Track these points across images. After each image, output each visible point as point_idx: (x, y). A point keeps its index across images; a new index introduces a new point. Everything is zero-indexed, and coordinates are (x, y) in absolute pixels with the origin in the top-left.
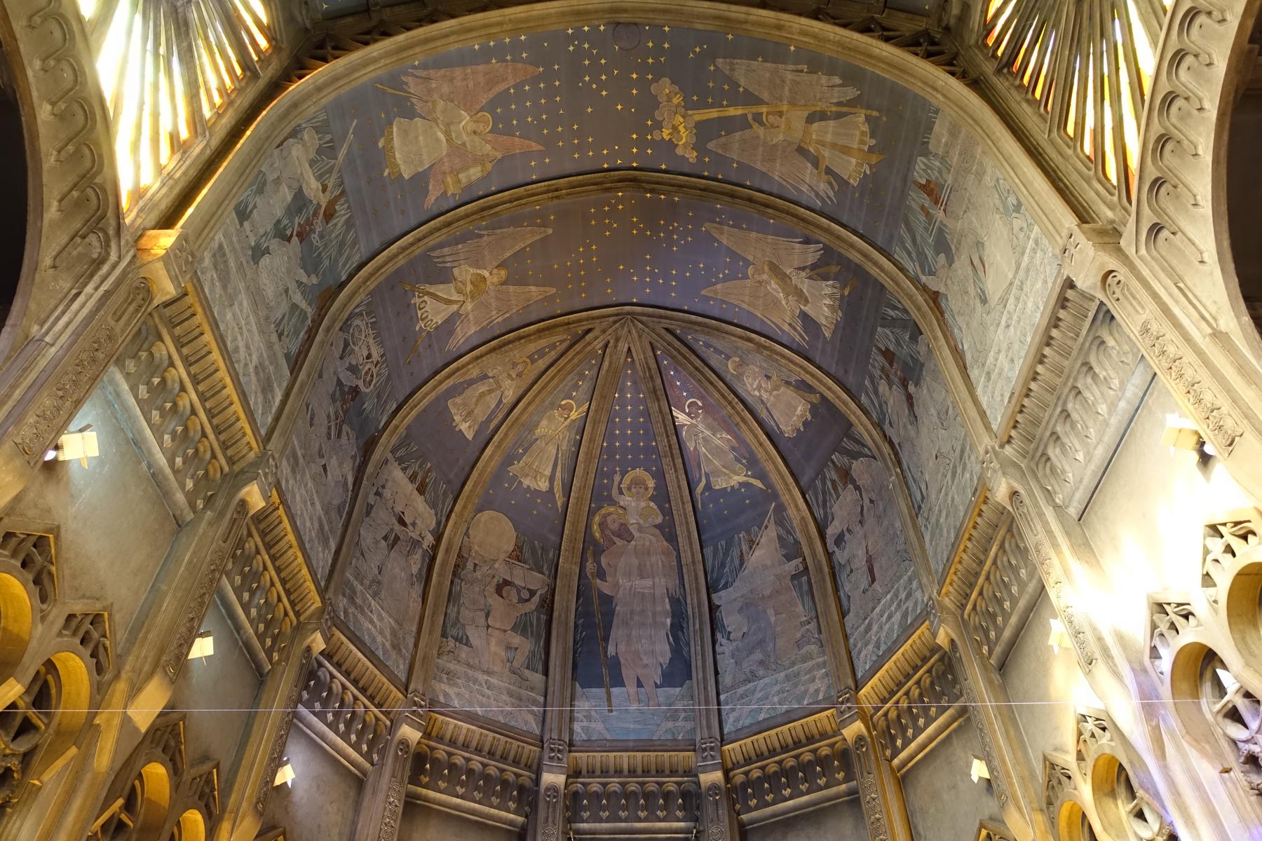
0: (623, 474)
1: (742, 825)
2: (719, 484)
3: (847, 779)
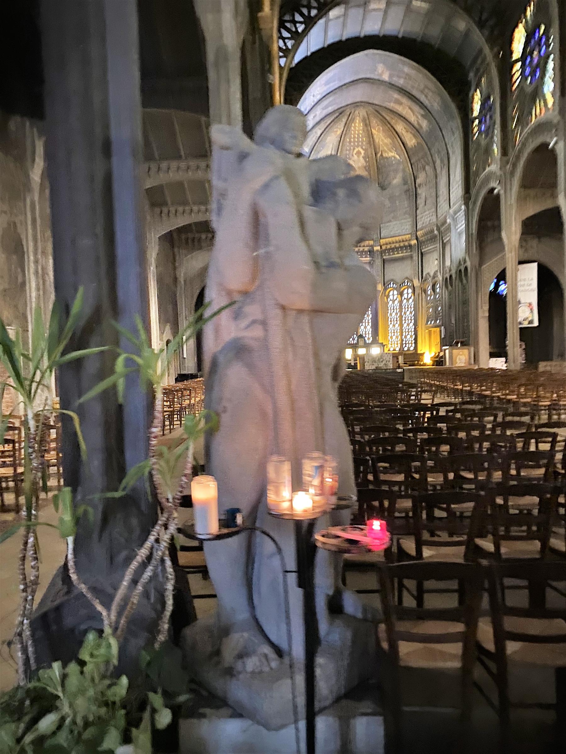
0: (354, 149)
1: (384, 260)
2: (385, 155)
3: (411, 251)
